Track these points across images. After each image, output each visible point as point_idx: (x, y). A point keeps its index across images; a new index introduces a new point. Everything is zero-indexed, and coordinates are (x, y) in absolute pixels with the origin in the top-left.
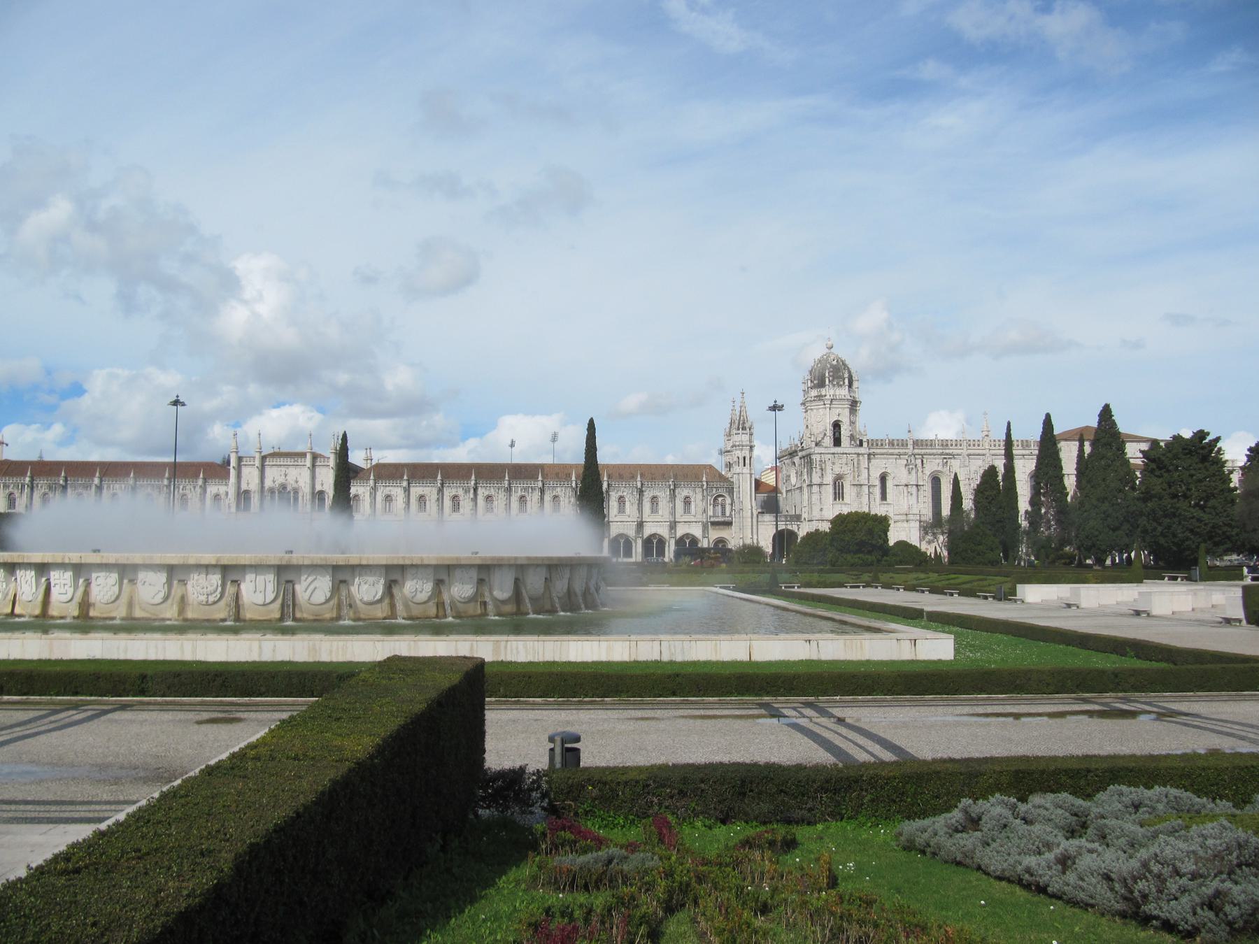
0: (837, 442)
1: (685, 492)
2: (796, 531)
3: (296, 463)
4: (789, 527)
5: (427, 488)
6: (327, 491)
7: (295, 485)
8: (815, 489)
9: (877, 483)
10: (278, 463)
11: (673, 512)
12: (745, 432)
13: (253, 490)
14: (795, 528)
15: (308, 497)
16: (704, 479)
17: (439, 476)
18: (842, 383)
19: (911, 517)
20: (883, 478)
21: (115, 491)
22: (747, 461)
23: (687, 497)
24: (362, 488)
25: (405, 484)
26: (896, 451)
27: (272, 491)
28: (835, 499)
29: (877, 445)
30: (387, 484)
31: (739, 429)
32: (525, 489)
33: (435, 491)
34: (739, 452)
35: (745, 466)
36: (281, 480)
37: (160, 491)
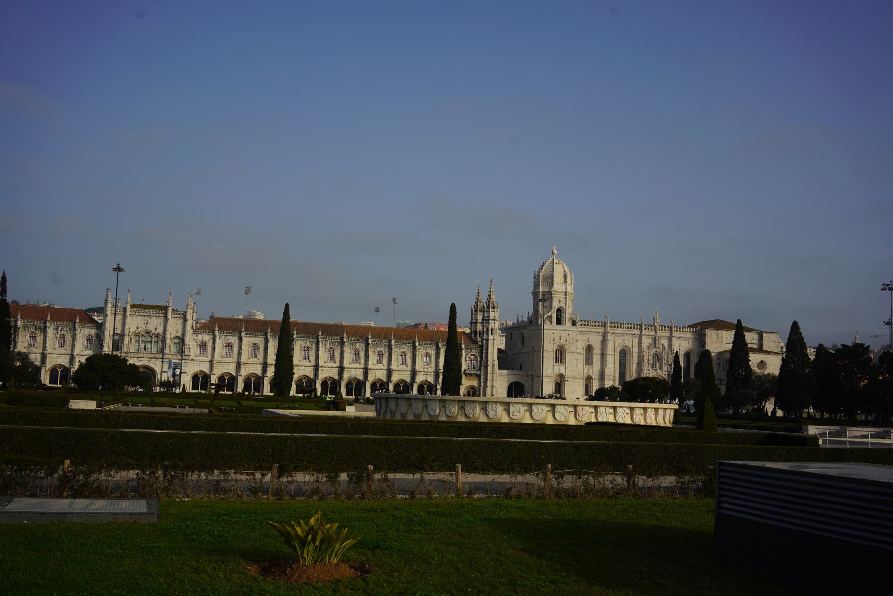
0: (559, 322)
5: (258, 339)
7: (157, 332)
9: (583, 352)
10: (143, 314)
12: (494, 310)
16: (463, 343)
22: (494, 332)
27: (138, 335)
28: (556, 362)
29: (585, 325)
30: (228, 334)
31: (488, 308)
32: (333, 343)
35: (491, 334)
36: (142, 327)
37: (41, 331)
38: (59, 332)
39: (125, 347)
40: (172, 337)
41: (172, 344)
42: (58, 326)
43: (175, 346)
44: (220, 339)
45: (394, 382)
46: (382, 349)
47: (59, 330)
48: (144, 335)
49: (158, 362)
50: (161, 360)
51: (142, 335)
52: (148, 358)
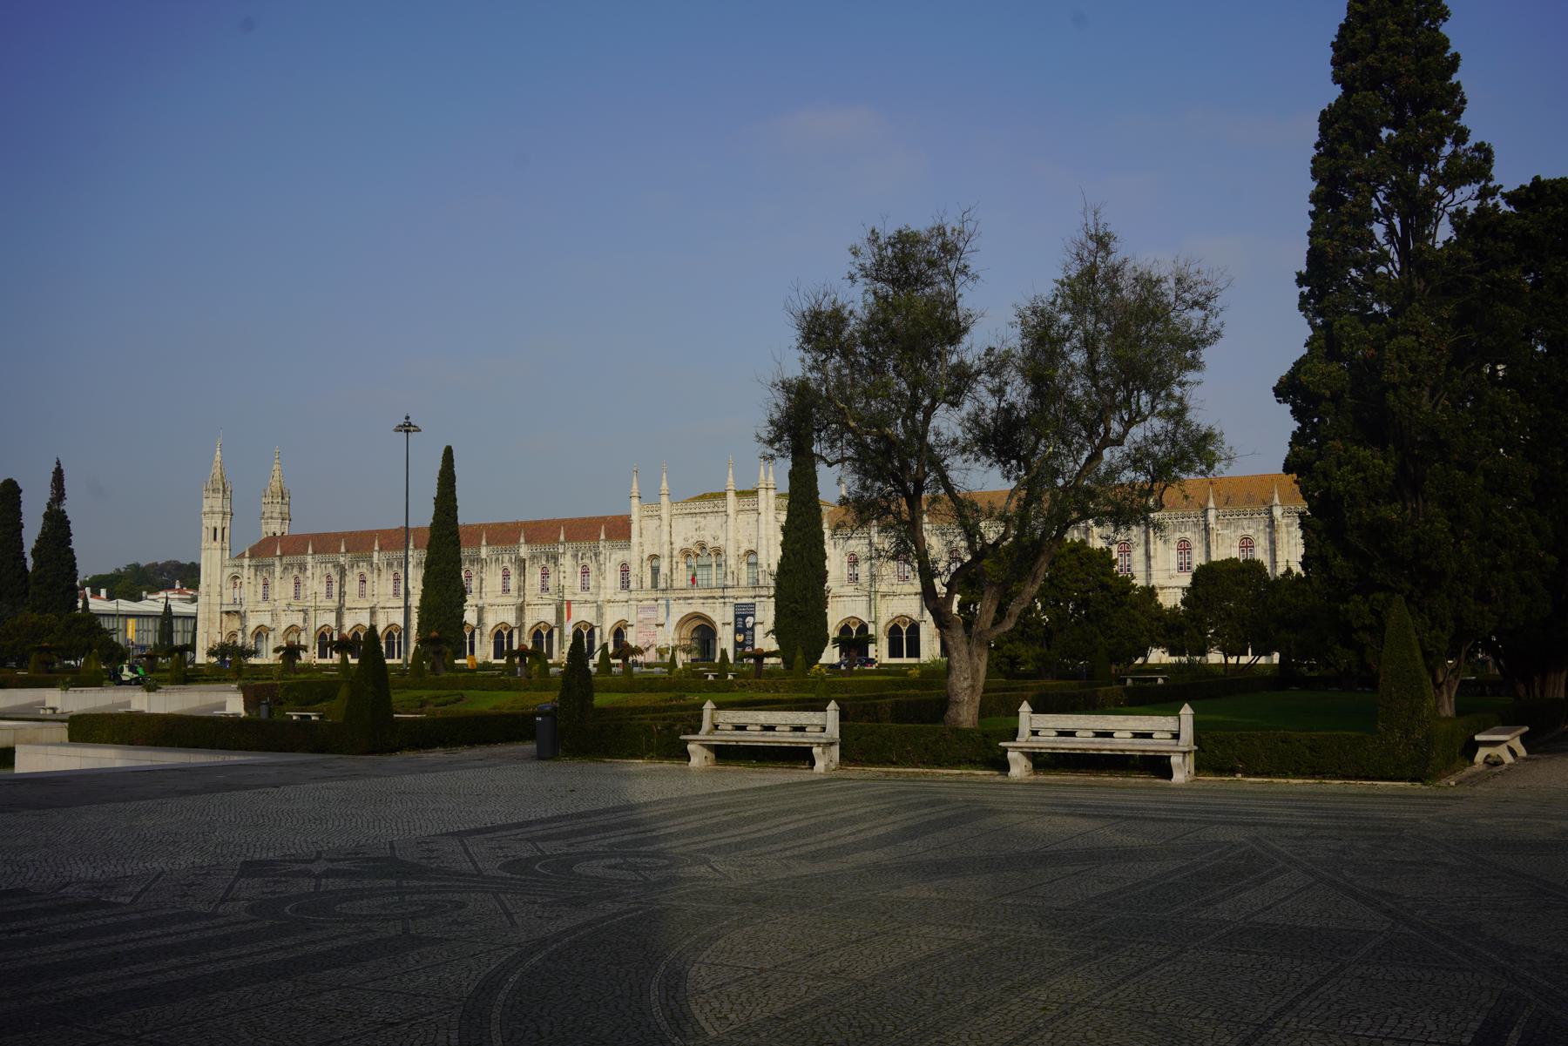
3: (716, 509)
10: (693, 511)
21: (504, 565)
27: (686, 553)
38: (580, 562)
39: (662, 581)
40: (742, 551)
41: (744, 566)
42: (577, 551)
43: (750, 571)
44: (835, 547)
46: (1188, 535)
47: (579, 558)
48: (698, 552)
49: (718, 605)
50: (723, 600)
51: (694, 552)
52: (701, 598)
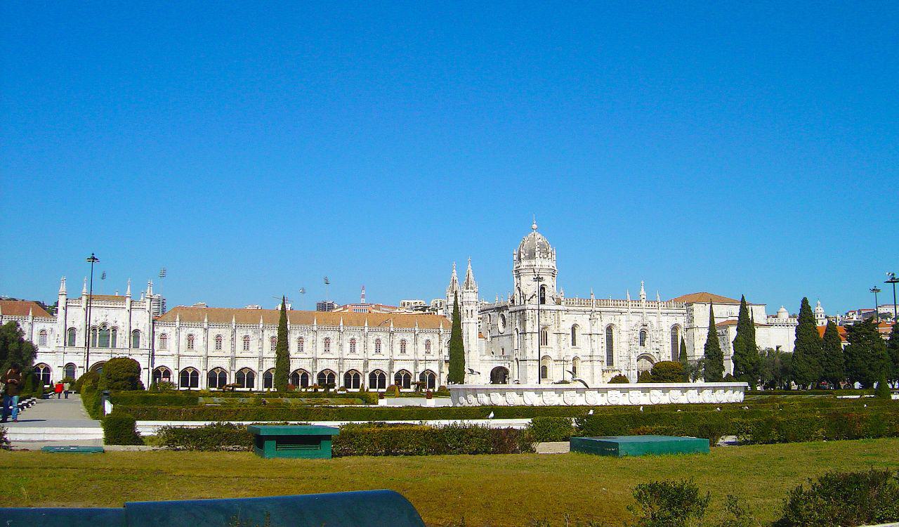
1: (426, 337)
2: (508, 368)
3: (115, 306)
4: (503, 365)
6: (142, 330)
7: (115, 325)
8: (528, 336)
9: (570, 332)
10: (100, 305)
11: (416, 353)
13: (78, 328)
14: (507, 366)
15: (128, 335)
17: (234, 319)
18: (546, 256)
19: (595, 358)
20: (573, 329)
23: (428, 341)
24: (169, 328)
25: (206, 326)
26: (583, 309)
33: (229, 332)
34: (467, 306)
36: (102, 320)
45: (370, 372)
